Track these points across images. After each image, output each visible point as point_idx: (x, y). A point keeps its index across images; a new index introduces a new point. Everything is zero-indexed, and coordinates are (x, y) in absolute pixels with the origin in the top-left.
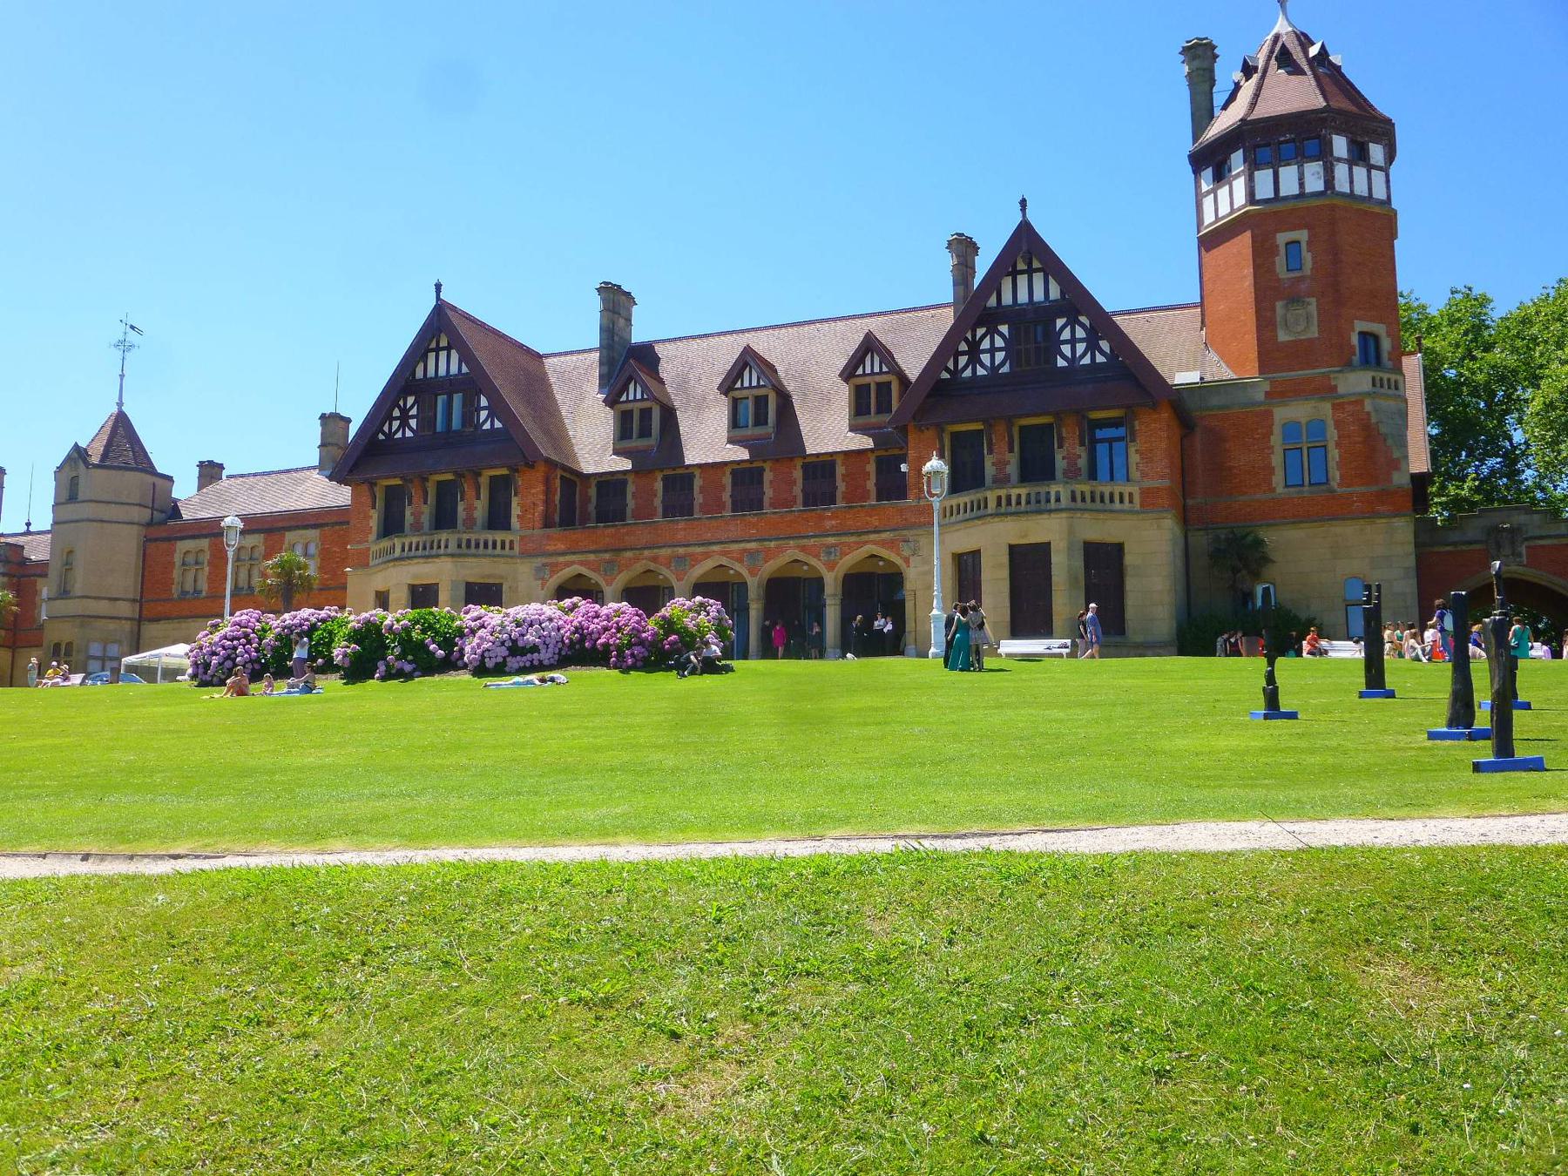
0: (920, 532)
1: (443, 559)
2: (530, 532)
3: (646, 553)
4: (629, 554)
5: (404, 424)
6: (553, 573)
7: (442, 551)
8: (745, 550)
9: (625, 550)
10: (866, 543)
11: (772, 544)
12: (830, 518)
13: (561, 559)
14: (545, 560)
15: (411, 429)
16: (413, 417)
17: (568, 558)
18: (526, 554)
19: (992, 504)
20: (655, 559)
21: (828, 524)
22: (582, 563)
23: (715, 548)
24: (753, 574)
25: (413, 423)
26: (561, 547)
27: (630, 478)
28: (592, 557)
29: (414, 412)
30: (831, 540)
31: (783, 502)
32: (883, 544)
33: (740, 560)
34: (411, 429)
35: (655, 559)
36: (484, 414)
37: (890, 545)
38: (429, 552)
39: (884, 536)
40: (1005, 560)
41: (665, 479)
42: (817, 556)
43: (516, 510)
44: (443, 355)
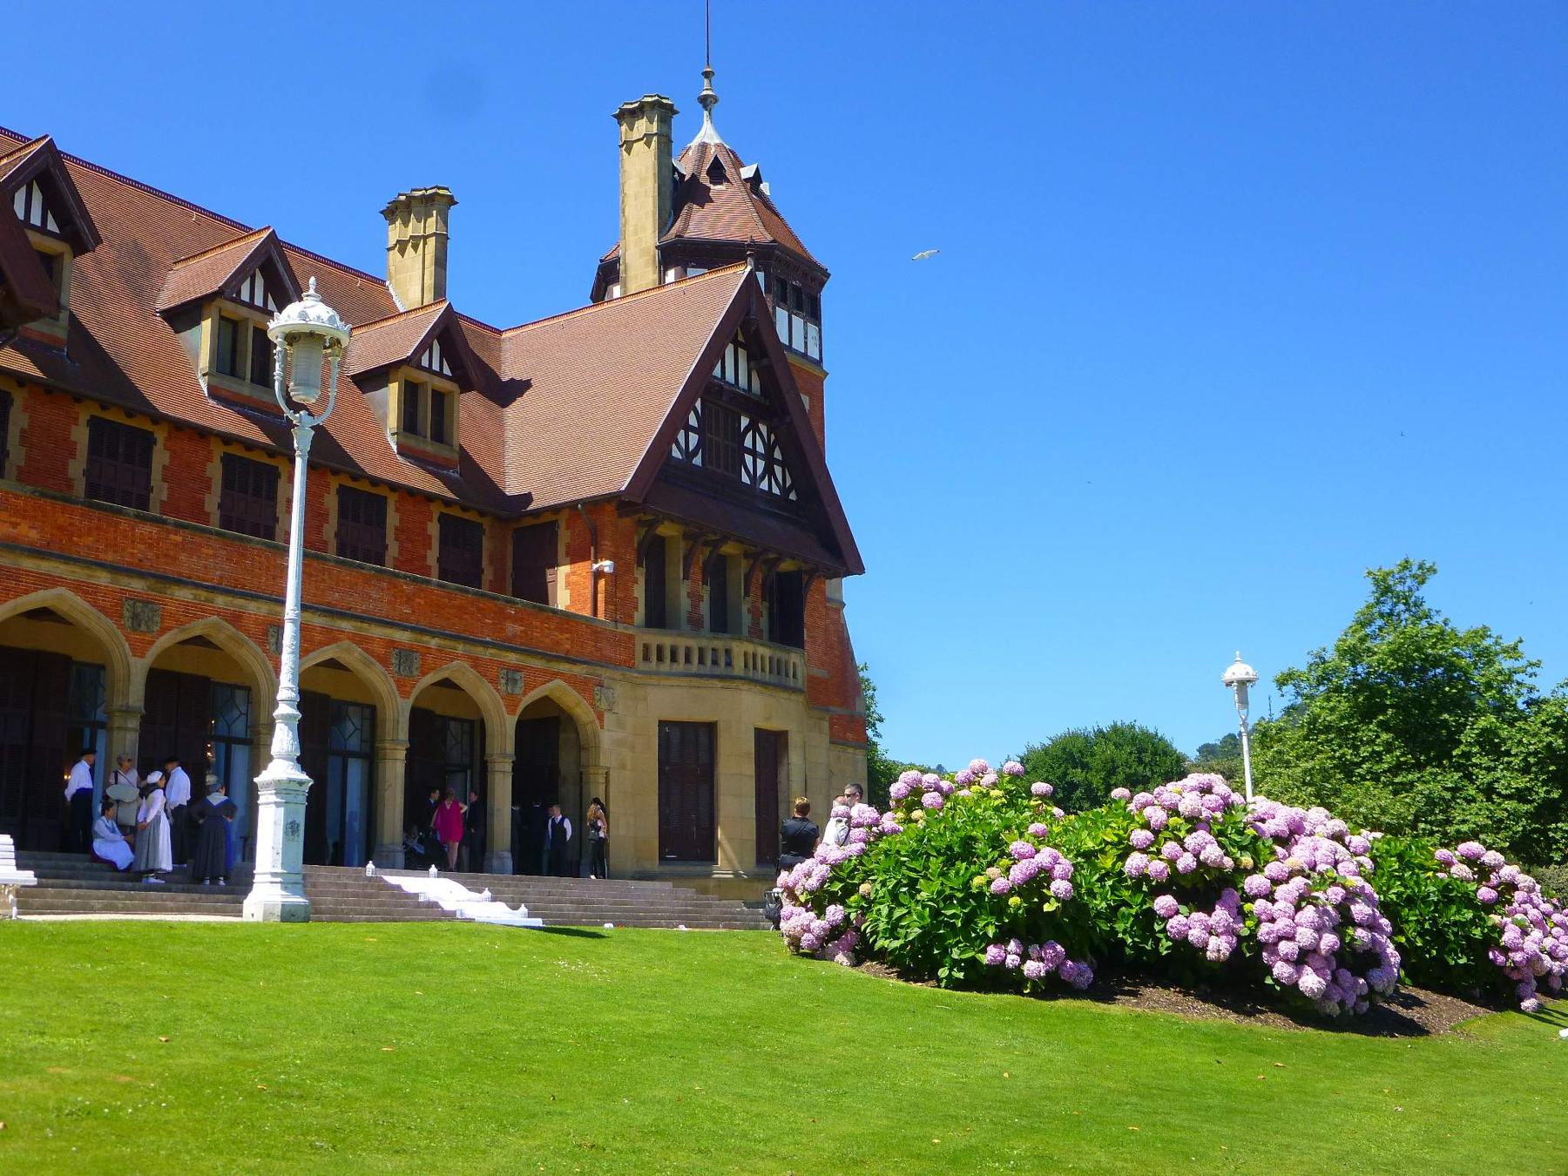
0: (617, 675)
3: (220, 601)
4: (185, 594)
8: (392, 643)
9: (179, 582)
10: (556, 675)
11: (434, 643)
12: (515, 620)
13: (28, 564)
17: (46, 566)
19: (739, 663)
20: (235, 618)
21: (513, 628)
22: (78, 587)
23: (346, 625)
24: (403, 688)
26: (29, 533)
27: (19, 397)
28: (103, 578)
30: (512, 658)
31: (412, 561)
32: (572, 680)
33: (384, 661)
35: (235, 618)
37: (583, 686)
39: (577, 670)
40: (750, 746)
41: (94, 423)
42: (494, 682)
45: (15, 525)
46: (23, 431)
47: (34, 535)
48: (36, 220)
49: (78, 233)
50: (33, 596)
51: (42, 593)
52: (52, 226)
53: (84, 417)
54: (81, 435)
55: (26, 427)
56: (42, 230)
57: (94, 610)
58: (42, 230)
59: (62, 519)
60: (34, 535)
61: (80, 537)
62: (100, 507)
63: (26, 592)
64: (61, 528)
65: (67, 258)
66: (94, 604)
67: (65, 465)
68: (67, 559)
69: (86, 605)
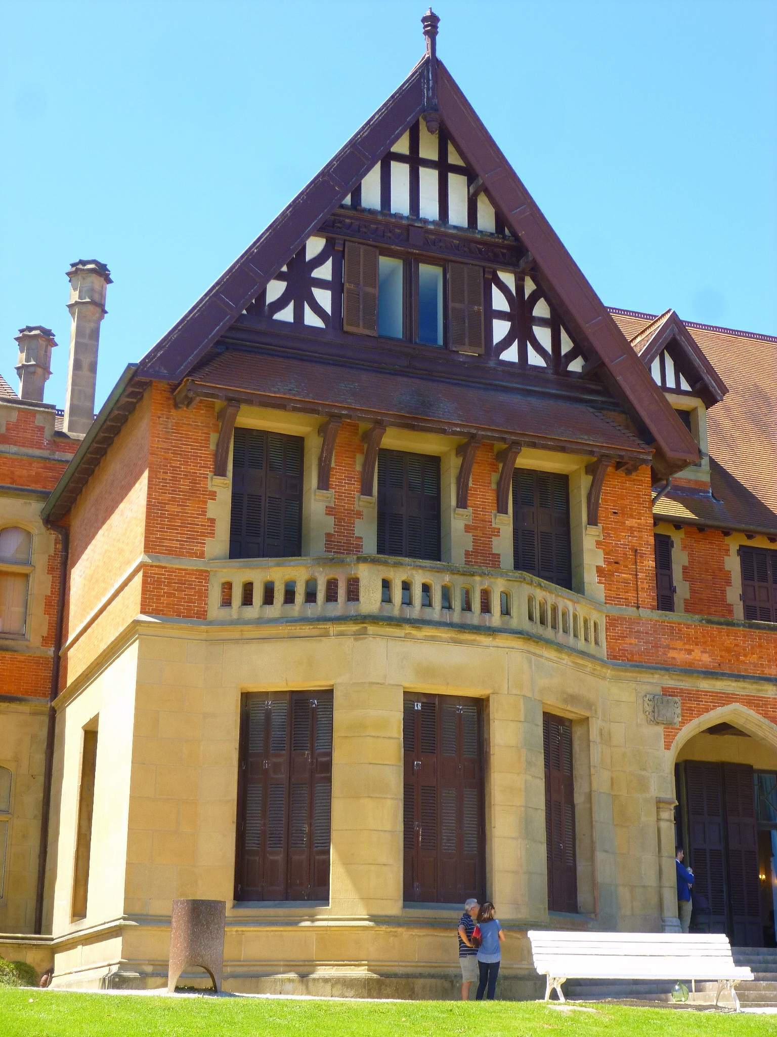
1: (503, 641)
2: (631, 612)
5: (300, 292)
6: (689, 714)
7: (496, 619)
13: (705, 685)
14: (670, 682)
15: (318, 310)
16: (322, 284)
17: (720, 685)
18: (623, 660)
22: (750, 702)
25: (324, 298)
29: (324, 272)
34: (318, 310)
36: (501, 329)
38: (468, 618)
41: (744, 552)
43: (591, 553)
44: (400, 173)
45: (690, 652)
46: (685, 568)
47: (706, 658)
48: (671, 383)
49: (707, 389)
50: (712, 714)
51: (720, 710)
52: (685, 386)
53: (734, 548)
54: (733, 564)
55: (687, 564)
56: (678, 391)
57: (767, 721)
58: (678, 391)
59: (729, 641)
60: (706, 658)
61: (745, 656)
62: (758, 627)
63: (707, 710)
64: (728, 650)
65: (701, 411)
66: (766, 716)
67: (723, 592)
68: (738, 677)
69: (759, 717)
